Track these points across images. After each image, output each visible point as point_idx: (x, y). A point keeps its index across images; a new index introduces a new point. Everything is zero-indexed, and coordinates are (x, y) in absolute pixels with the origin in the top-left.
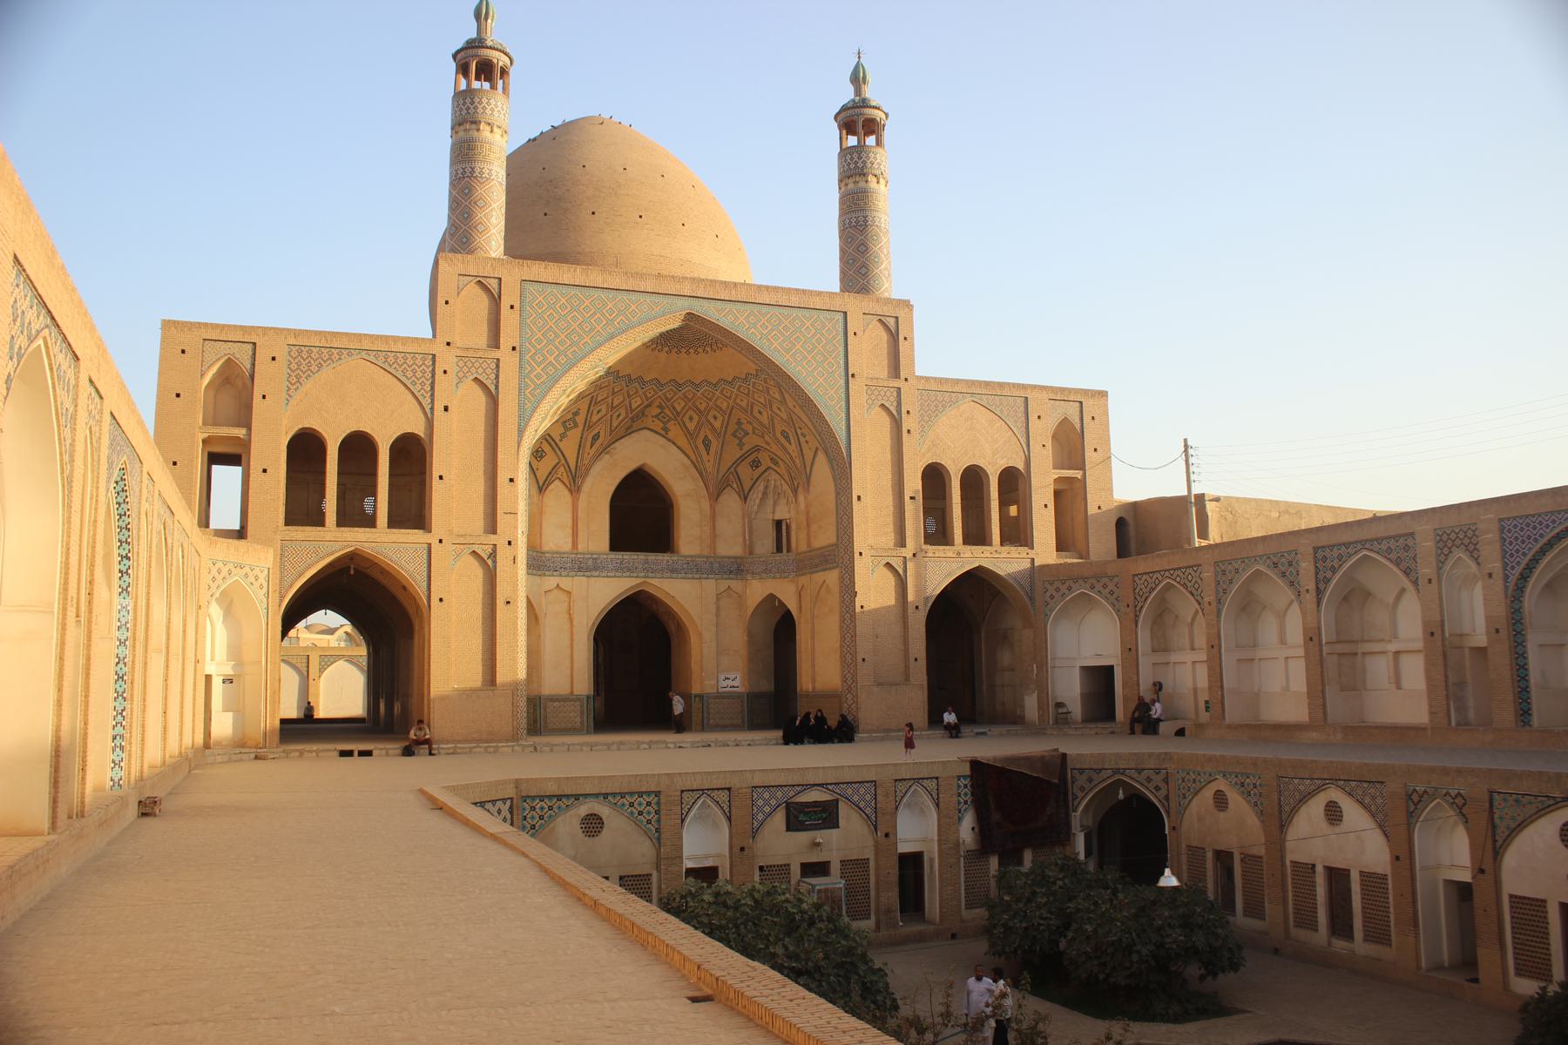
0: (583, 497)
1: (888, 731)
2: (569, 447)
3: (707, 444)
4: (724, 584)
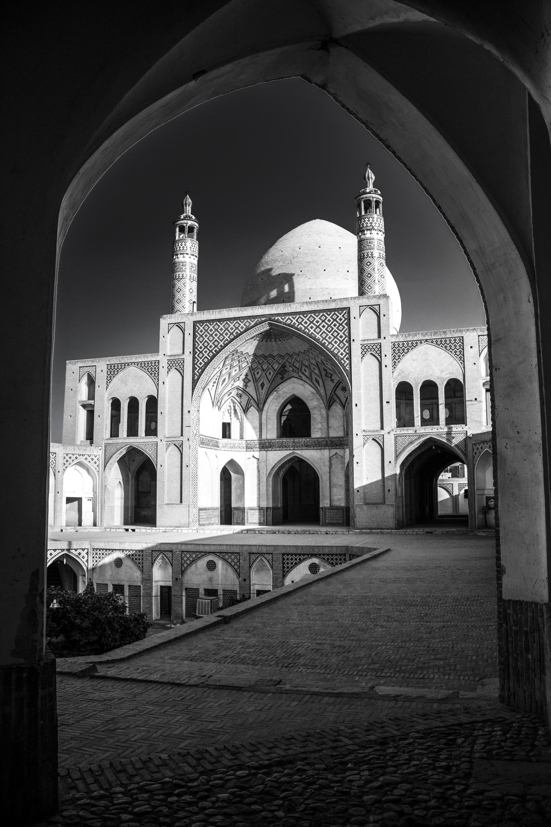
0: (264, 413)
1: (371, 529)
2: (251, 389)
3: (318, 383)
4: (333, 452)
